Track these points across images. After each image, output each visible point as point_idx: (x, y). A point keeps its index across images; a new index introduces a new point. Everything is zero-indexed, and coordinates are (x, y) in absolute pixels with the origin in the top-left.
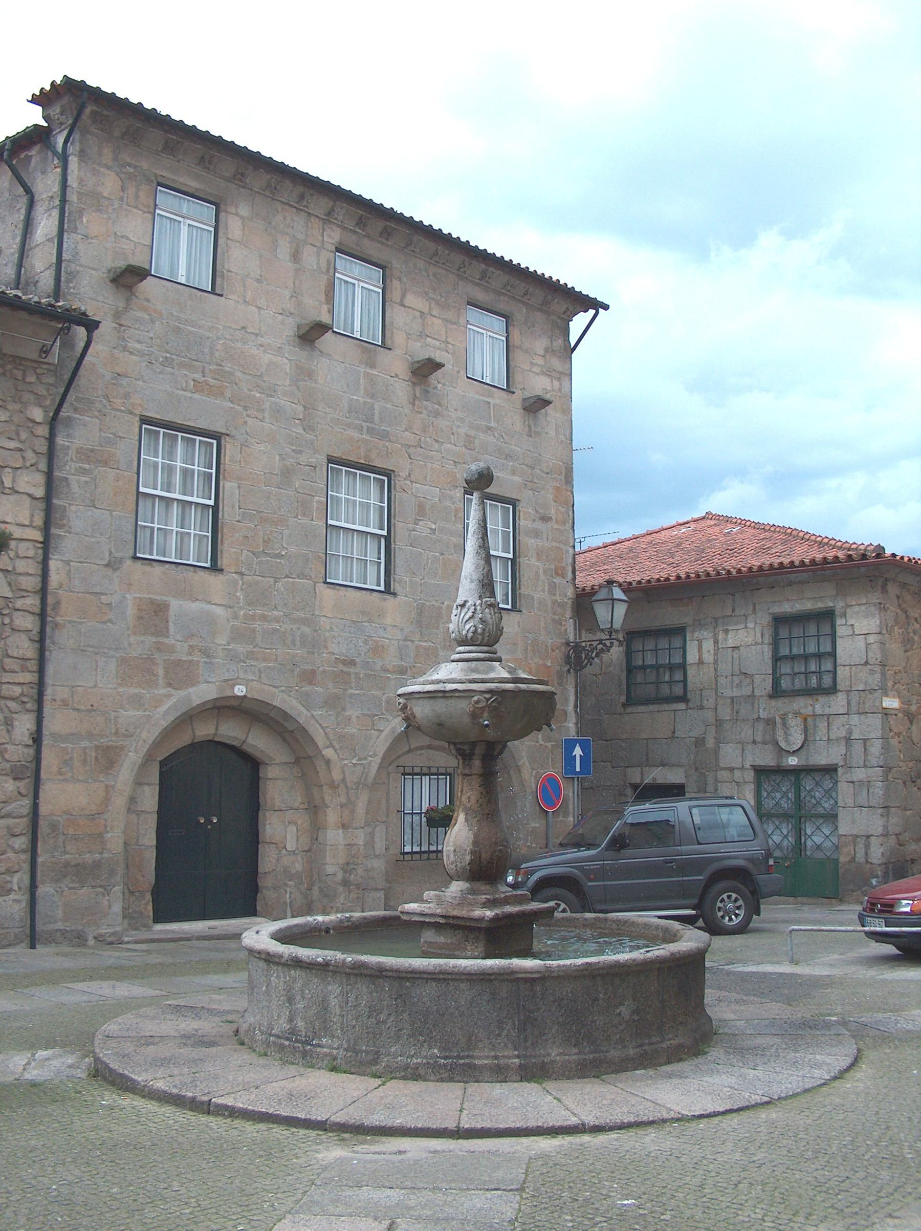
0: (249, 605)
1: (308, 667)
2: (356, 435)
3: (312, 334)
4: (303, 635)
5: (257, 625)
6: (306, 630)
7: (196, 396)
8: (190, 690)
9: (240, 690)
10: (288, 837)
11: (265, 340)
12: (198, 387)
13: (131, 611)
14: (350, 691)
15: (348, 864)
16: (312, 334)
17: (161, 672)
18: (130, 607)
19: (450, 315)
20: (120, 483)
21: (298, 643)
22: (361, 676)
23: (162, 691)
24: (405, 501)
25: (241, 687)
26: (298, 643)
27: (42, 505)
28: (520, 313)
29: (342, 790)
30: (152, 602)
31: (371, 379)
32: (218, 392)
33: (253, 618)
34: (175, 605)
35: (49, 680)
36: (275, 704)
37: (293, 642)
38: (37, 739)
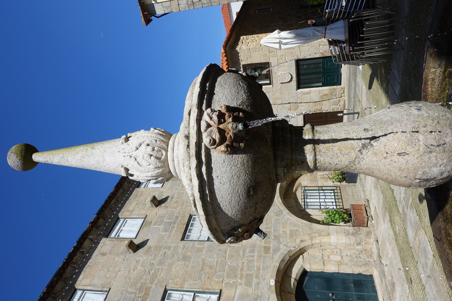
0: (236, 276)
1: (263, 249)
2: (175, 228)
4: (250, 252)
5: (245, 273)
6: (248, 250)
9: (273, 282)
10: (335, 259)
11: (132, 268)
14: (272, 231)
15: (345, 233)
19: (139, 194)
21: (253, 254)
22: (266, 226)
25: (271, 282)
26: (253, 254)
29: (313, 235)
32: (148, 289)
33: (242, 275)
36: (278, 265)
37: (252, 256)
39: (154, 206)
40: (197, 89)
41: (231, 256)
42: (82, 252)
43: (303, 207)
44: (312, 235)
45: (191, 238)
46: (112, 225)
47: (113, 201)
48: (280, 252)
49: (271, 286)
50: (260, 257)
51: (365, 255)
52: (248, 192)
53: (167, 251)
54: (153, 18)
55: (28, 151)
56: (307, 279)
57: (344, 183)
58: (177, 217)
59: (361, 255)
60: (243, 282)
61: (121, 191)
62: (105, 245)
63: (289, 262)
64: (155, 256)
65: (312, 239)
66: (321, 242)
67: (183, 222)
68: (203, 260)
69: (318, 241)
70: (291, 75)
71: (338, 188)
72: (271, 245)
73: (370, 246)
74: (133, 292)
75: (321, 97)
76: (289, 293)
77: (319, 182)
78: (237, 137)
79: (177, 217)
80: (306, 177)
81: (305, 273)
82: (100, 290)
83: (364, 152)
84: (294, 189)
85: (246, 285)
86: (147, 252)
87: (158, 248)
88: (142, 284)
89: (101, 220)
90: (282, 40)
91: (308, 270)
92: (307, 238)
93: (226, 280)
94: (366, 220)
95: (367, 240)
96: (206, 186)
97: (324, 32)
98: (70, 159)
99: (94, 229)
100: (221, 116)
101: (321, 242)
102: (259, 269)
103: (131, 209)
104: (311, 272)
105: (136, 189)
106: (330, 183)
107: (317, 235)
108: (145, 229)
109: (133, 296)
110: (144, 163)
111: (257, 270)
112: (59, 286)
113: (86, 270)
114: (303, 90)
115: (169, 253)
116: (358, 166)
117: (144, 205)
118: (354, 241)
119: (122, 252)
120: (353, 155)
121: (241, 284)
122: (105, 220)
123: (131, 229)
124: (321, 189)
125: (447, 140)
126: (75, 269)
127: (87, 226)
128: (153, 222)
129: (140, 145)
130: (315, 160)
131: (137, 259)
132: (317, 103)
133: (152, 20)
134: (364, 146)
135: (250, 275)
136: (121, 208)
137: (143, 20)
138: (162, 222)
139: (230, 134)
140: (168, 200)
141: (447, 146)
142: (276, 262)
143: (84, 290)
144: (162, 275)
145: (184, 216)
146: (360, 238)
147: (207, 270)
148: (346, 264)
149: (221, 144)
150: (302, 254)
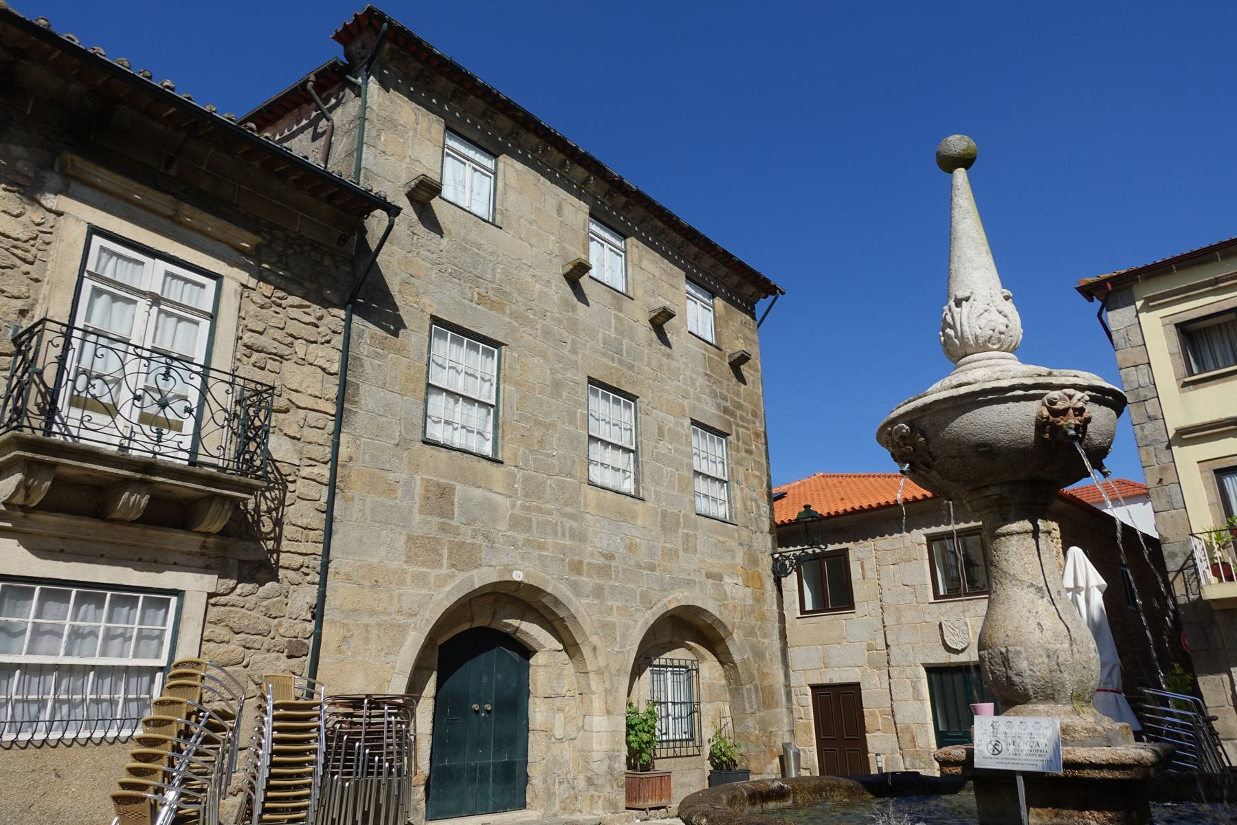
0: (526, 496)
1: (577, 558)
4: (571, 528)
5: (533, 515)
6: (575, 525)
8: (474, 572)
9: (518, 576)
11: (537, 273)
12: (482, 300)
13: (418, 491)
14: (611, 583)
17: (445, 553)
18: (418, 488)
20: (412, 371)
23: (444, 571)
27: (336, 380)
29: (606, 676)
32: (500, 307)
33: (528, 509)
34: (459, 488)
35: (333, 554)
37: (563, 534)
38: (318, 613)
39: (653, 314)
40: (1107, 385)
41: (562, 487)
42: (563, 165)
43: (656, 662)
44: (606, 674)
45: (591, 398)
46: (613, 225)
47: (660, 224)
48: (573, 598)
49: (511, 571)
50: (563, 550)
51: (566, 796)
52: (984, 445)
53: (569, 346)
54: (1097, 304)
55: (966, 161)
56: (516, 656)
57: (708, 767)
58: (631, 367)
59: (566, 785)
60: (517, 511)
61: (680, 239)
62: (577, 210)
63: (550, 618)
64: (559, 321)
65: (599, 672)
66: (593, 693)
67: (623, 381)
68: (552, 426)
69: (594, 686)
70: (963, 650)
71: (696, 752)
72: (585, 578)
73: (586, 809)
74: (494, 275)
75: (908, 728)
76: (494, 614)
77: (709, 706)
78: (1056, 429)
79: (631, 367)
80: (717, 675)
81: (527, 652)
82: (498, 207)
83: (1032, 589)
84: (693, 644)
85: (513, 517)
86: (566, 303)
87: (573, 326)
88: (509, 294)
89: (624, 199)
90: (1083, 593)
91: (531, 662)
92: (602, 662)
93: (519, 475)
94: (640, 804)
95: (600, 802)
96: (998, 395)
97: (1109, 687)
98: (968, 221)
99: (607, 186)
100: (1082, 410)
101: (593, 693)
102: (541, 547)
103: (646, 264)
104: (529, 666)
105: (683, 274)
106: (708, 733)
107: (608, 685)
108: (607, 297)
109: (489, 277)
110: (983, 322)
111: (540, 543)
112: (504, 122)
113: (531, 176)
114: (925, 681)
115: (565, 351)
116: (1009, 585)
117: (653, 294)
118: (597, 771)
119: (563, 249)
120: (1025, 577)
121: (513, 506)
122: (623, 208)
123: (606, 267)
124: (693, 708)
125: (1066, 675)
126: (534, 151)
127: (616, 170)
128: (622, 315)
129: (1005, 316)
130: (1011, 534)
131: (554, 283)
132: (890, 717)
133: (1091, 300)
134: (1039, 590)
135: (530, 528)
136: (645, 241)
137: (1090, 280)
138: (621, 333)
139: (1061, 421)
140: (663, 347)
141: (1058, 674)
142: (555, 587)
143: (495, 174)
144: (526, 337)
145: (634, 383)
146: (603, 786)
147: (537, 434)
148: (548, 749)
149: (1050, 410)
150: (566, 649)
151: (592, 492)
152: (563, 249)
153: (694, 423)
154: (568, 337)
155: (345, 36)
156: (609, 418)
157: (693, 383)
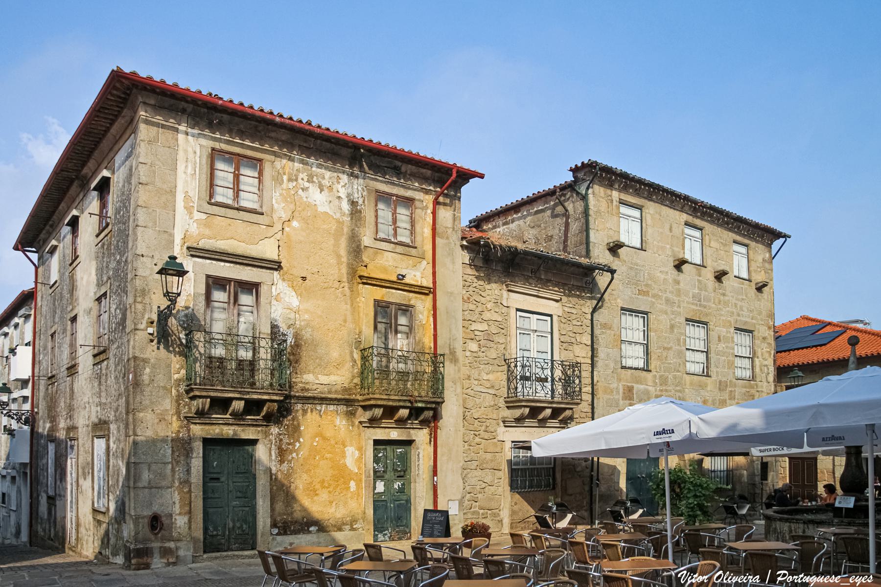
3: (680, 265)
7: (640, 297)
11: (662, 269)
13: (621, 391)
16: (680, 265)
24: (714, 335)
28: (753, 244)
30: (628, 387)
31: (699, 281)
34: (636, 386)
41: (675, 377)
119: (673, 251)
138: (700, 289)
145: (707, 315)
151: (688, 377)
152: (673, 251)
153: (737, 329)
154: (676, 299)
155: (575, 170)
156: (696, 333)
157: (736, 306)
